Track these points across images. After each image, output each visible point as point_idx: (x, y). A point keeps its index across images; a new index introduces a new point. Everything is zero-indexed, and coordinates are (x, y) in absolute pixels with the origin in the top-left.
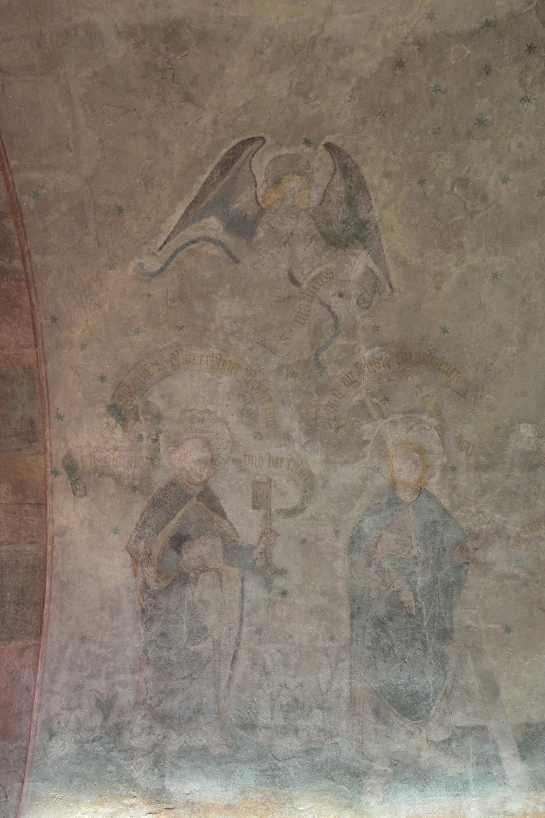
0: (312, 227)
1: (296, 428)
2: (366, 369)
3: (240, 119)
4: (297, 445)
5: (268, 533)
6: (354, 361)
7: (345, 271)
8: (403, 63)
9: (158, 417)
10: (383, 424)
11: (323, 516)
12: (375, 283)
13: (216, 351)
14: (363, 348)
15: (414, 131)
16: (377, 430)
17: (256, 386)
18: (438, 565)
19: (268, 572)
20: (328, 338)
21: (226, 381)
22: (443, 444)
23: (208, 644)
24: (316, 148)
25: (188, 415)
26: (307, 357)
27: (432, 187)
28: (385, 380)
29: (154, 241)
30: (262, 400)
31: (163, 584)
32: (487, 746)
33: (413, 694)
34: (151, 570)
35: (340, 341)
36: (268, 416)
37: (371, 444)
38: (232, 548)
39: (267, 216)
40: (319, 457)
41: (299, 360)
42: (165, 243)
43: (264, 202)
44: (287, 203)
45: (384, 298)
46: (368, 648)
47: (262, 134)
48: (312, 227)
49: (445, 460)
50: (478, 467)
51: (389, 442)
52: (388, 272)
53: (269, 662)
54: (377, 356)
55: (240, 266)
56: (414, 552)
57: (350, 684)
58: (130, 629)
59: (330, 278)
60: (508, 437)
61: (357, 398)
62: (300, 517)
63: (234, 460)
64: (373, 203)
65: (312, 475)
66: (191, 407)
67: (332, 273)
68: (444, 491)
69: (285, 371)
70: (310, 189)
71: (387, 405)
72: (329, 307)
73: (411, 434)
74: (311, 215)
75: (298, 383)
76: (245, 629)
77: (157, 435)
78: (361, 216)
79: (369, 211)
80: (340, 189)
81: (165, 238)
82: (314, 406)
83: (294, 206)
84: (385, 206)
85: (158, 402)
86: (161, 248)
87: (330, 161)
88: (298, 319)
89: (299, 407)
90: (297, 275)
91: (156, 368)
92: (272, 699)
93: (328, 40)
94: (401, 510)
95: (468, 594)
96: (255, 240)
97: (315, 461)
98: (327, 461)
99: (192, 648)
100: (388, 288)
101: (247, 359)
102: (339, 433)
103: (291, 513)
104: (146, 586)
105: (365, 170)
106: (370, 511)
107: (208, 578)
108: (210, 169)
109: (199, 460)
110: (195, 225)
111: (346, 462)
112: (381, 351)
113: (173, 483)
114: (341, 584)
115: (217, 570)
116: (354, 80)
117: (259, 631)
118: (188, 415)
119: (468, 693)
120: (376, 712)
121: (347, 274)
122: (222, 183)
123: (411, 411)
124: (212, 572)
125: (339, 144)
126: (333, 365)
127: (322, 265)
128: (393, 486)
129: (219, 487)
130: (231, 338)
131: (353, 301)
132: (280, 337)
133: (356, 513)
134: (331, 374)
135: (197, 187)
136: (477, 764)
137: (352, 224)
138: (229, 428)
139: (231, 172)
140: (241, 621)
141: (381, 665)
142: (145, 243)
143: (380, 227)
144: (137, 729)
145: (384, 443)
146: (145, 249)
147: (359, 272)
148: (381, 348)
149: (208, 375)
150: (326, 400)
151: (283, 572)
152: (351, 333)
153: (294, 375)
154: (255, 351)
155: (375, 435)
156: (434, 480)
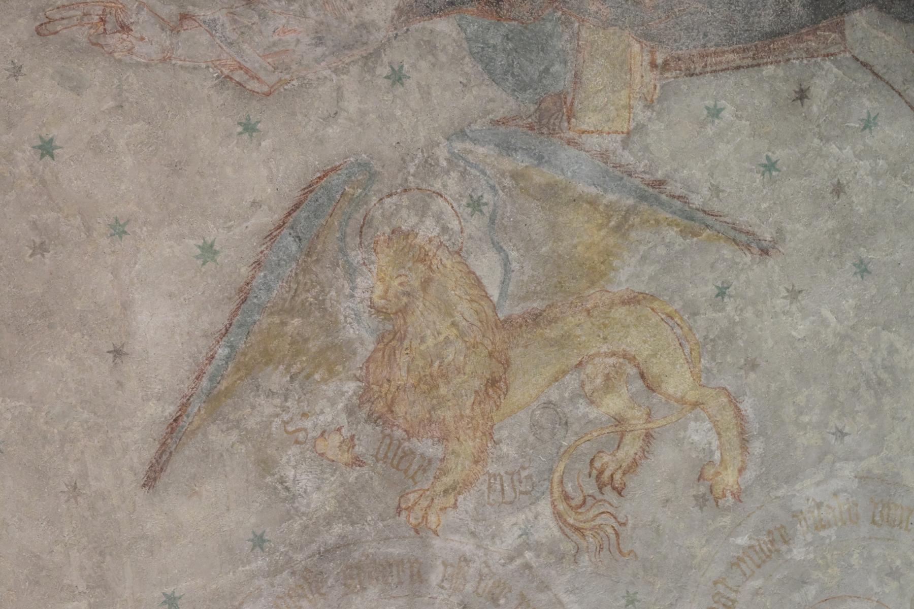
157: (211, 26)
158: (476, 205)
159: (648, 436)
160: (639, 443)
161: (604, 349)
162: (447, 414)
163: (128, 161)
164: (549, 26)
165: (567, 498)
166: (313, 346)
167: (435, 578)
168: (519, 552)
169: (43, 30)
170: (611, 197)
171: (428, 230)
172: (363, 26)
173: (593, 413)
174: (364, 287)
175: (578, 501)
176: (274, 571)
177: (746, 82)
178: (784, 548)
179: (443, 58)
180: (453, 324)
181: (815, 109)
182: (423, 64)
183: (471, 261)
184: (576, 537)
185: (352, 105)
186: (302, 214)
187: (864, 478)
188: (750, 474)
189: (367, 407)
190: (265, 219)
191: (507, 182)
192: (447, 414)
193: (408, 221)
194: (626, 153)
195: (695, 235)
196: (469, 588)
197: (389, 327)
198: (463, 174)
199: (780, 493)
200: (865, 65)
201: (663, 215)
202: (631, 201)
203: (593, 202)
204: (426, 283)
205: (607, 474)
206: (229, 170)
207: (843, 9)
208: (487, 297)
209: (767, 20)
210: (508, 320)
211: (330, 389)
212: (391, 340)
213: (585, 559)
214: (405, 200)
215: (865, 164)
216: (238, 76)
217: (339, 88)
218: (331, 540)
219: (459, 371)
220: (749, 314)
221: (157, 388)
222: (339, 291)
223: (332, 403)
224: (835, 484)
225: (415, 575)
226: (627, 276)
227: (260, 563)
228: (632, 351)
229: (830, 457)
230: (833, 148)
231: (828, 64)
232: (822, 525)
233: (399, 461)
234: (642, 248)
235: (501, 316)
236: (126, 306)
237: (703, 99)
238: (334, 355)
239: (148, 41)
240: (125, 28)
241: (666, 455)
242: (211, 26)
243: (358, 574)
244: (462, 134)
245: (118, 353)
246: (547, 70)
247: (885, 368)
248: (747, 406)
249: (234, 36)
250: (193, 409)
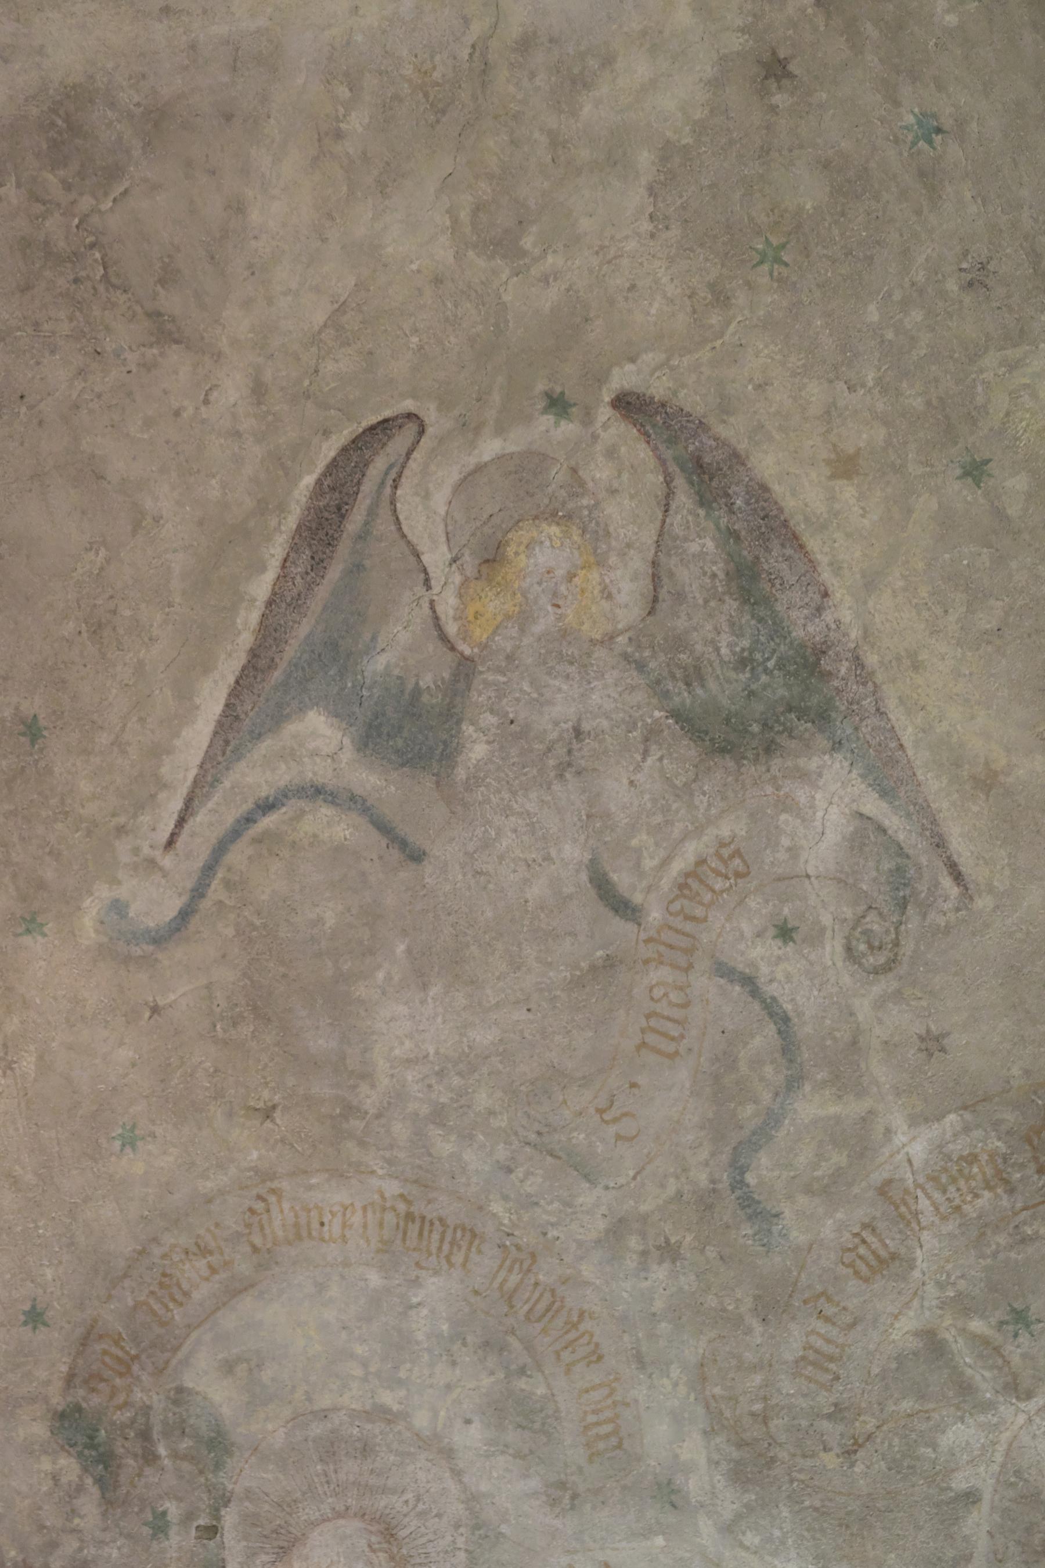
0: (639, 697)
1: (694, 1456)
2: (924, 1203)
3: (329, 367)
4: (706, 1527)
6: (877, 1177)
7: (785, 842)
8: (783, 63)
9: (217, 1445)
10: (1021, 1419)
12: (899, 870)
13: (392, 1188)
14: (898, 1121)
15: (897, 296)
16: (1001, 1448)
17: (542, 1306)
20: (766, 1097)
21: (437, 1295)
24: (587, 419)
26: (702, 1178)
27: (1019, 483)
28: (1002, 1239)
29: (145, 819)
30: (566, 1356)
35: (811, 1107)
36: (591, 1418)
37: (985, 1506)
39: (485, 682)
41: (679, 1195)
42: (181, 822)
43: (465, 635)
44: (538, 629)
45: (942, 921)
47: (408, 405)
48: (639, 697)
52: (934, 822)
54: (959, 1147)
55: (428, 868)
59: (738, 875)
61: (908, 1323)
64: (826, 575)
66: (325, 1401)
67: (737, 853)
69: (634, 1242)
70: (602, 565)
71: (1024, 1339)
72: (749, 982)
74: (625, 656)
75: (688, 1281)
78: (798, 633)
79: (819, 610)
80: (702, 545)
81: (176, 805)
82: (754, 1368)
84: (871, 583)
85: (217, 1394)
86: (170, 843)
87: (643, 452)
88: (651, 1038)
89: (700, 1376)
90: (622, 879)
91: (201, 1264)
93: (526, 44)
96: (461, 773)
100: (946, 881)
101: (497, 1207)
102: (859, 1468)
105: (766, 464)
108: (276, 550)
110: (266, 746)
112: (967, 1129)
116: (645, 159)
118: (317, 1429)
121: (793, 852)
122: (322, 592)
125: (659, 388)
126: (802, 1200)
127: (699, 830)
130: (434, 1132)
131: (833, 949)
132: (600, 1111)
134: (799, 1237)
137: (770, 664)
138: (457, 1474)
139: (344, 549)
142: (121, 830)
143: (871, 659)
146: (123, 849)
147: (832, 837)
148: (968, 1116)
149: (375, 1279)
150: (794, 1340)
152: (845, 1067)
153: (670, 1252)
154: (520, 1172)
155: (996, 1468)
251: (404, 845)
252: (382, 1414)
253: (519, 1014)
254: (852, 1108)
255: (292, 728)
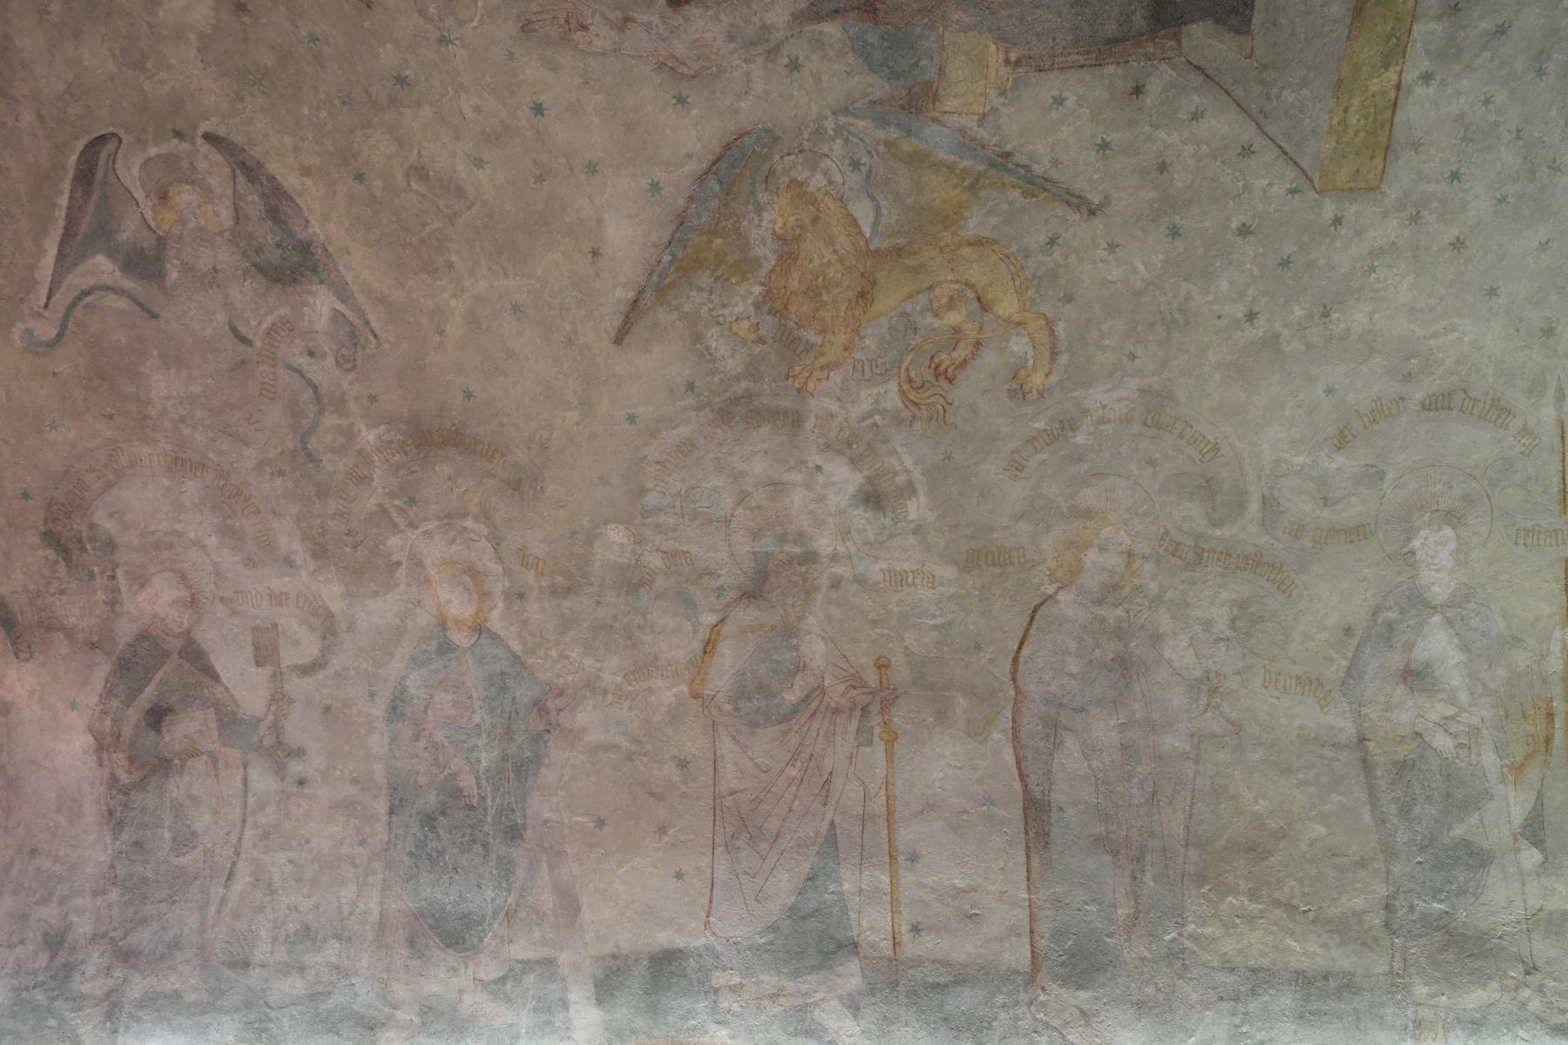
0: (238, 257)
4: (304, 575)
5: (278, 699)
6: (358, 447)
8: (244, 5)
9: (110, 545)
11: (352, 673)
12: (352, 332)
13: (168, 447)
14: (362, 427)
18: (508, 735)
19: (280, 753)
22: (500, 560)
23: (197, 855)
24: (193, 142)
25: (150, 538)
27: (378, 183)
29: (32, 296)
31: (137, 775)
32: (553, 987)
33: (463, 917)
34: (120, 758)
35: (329, 420)
38: (230, 723)
40: (337, 588)
42: (49, 298)
43: (159, 227)
46: (410, 854)
47: (112, 129)
49: (507, 584)
50: (554, 592)
51: (428, 562)
53: (277, 878)
54: (386, 438)
56: (477, 718)
57: (382, 903)
58: (93, 837)
60: (591, 545)
61: (372, 501)
62: (321, 675)
63: (223, 600)
65: (331, 615)
66: (152, 528)
68: (512, 629)
72: (300, 372)
73: (453, 548)
75: (289, 484)
76: (248, 833)
77: (114, 570)
81: (44, 291)
83: (202, 229)
84: (325, 218)
85: (109, 526)
86: (46, 307)
87: (220, 158)
90: (243, 329)
92: (275, 927)
94: (456, 659)
95: (548, 776)
97: (332, 593)
98: (349, 594)
99: (175, 861)
101: (211, 455)
103: (307, 670)
104: (114, 778)
105: (273, 167)
106: (417, 662)
107: (199, 764)
108: (66, 186)
109: (176, 601)
110: (81, 268)
111: (375, 595)
113: (144, 636)
114: (378, 767)
115: (211, 754)
117: (266, 835)
118: (150, 538)
119: (537, 913)
120: (412, 943)
121: (310, 322)
122: (91, 205)
123: (449, 516)
124: (205, 757)
125: (221, 132)
127: (271, 312)
128: (443, 624)
129: (208, 638)
130: (182, 426)
131: (330, 361)
133: (396, 666)
134: (330, 468)
135: (61, 214)
136: (535, 1010)
138: (208, 555)
140: (244, 821)
141: (425, 878)
142: (22, 300)
143: (330, 249)
144: (90, 971)
145: (420, 564)
146: (25, 307)
149: (167, 482)
150: (332, 506)
151: (300, 753)
152: (340, 407)
153: (281, 473)
156: (495, 614)
157: (648, 27)
158: (856, 165)
159: (978, 344)
160: (970, 348)
161: (950, 277)
162: (827, 314)
163: (596, 121)
164: (918, 30)
165: (910, 381)
166: (731, 259)
167: (809, 424)
168: (870, 415)
169: (526, 28)
170: (966, 163)
171: (817, 182)
172: (765, 27)
173: (937, 323)
174: (769, 220)
175: (919, 383)
176: (699, 408)
177: (1089, 78)
178: (1070, 434)
179: (830, 53)
180: (835, 251)
181: (1148, 101)
182: (815, 57)
183: (852, 208)
184: (913, 408)
185: (759, 86)
186: (722, 165)
187: (1144, 391)
188: (1054, 378)
189: (769, 304)
190: (695, 167)
191: (881, 148)
192: (827, 314)
193: (802, 174)
194: (981, 130)
195: (1034, 196)
196: (832, 434)
197: (786, 249)
198: (846, 141)
199: (1076, 394)
200: (1197, 68)
201: (1009, 179)
202: (982, 167)
203: (951, 167)
204: (815, 221)
205: (942, 368)
206: (668, 131)
207: (1181, 20)
208: (861, 233)
209: (1110, 28)
210: (877, 251)
211: (742, 289)
212: (788, 258)
213: (918, 425)
214: (800, 159)
215: (1190, 148)
216: (670, 63)
217: (748, 74)
218: (740, 392)
219: (837, 285)
220: (1073, 259)
221: (622, 279)
222: (751, 221)
223: (743, 300)
224: (1121, 393)
225: (795, 421)
226: (973, 225)
227: (690, 401)
228: (973, 280)
229: (1120, 373)
230: (1163, 135)
231: (1164, 66)
232: (1103, 421)
233: (789, 343)
234: (989, 204)
235: (872, 247)
236: (599, 221)
237: (1050, 90)
238: (746, 267)
239: (602, 37)
240: (584, 28)
241: (990, 360)
242: (648, 27)
243: (757, 416)
244: (845, 111)
245: (595, 253)
246: (916, 64)
247: (1179, 310)
248: (1060, 329)
249: (665, 34)
250: (647, 295)
251: (149, 311)
252: (176, 533)
253: (209, 381)
254: (345, 422)
255: (91, 261)
